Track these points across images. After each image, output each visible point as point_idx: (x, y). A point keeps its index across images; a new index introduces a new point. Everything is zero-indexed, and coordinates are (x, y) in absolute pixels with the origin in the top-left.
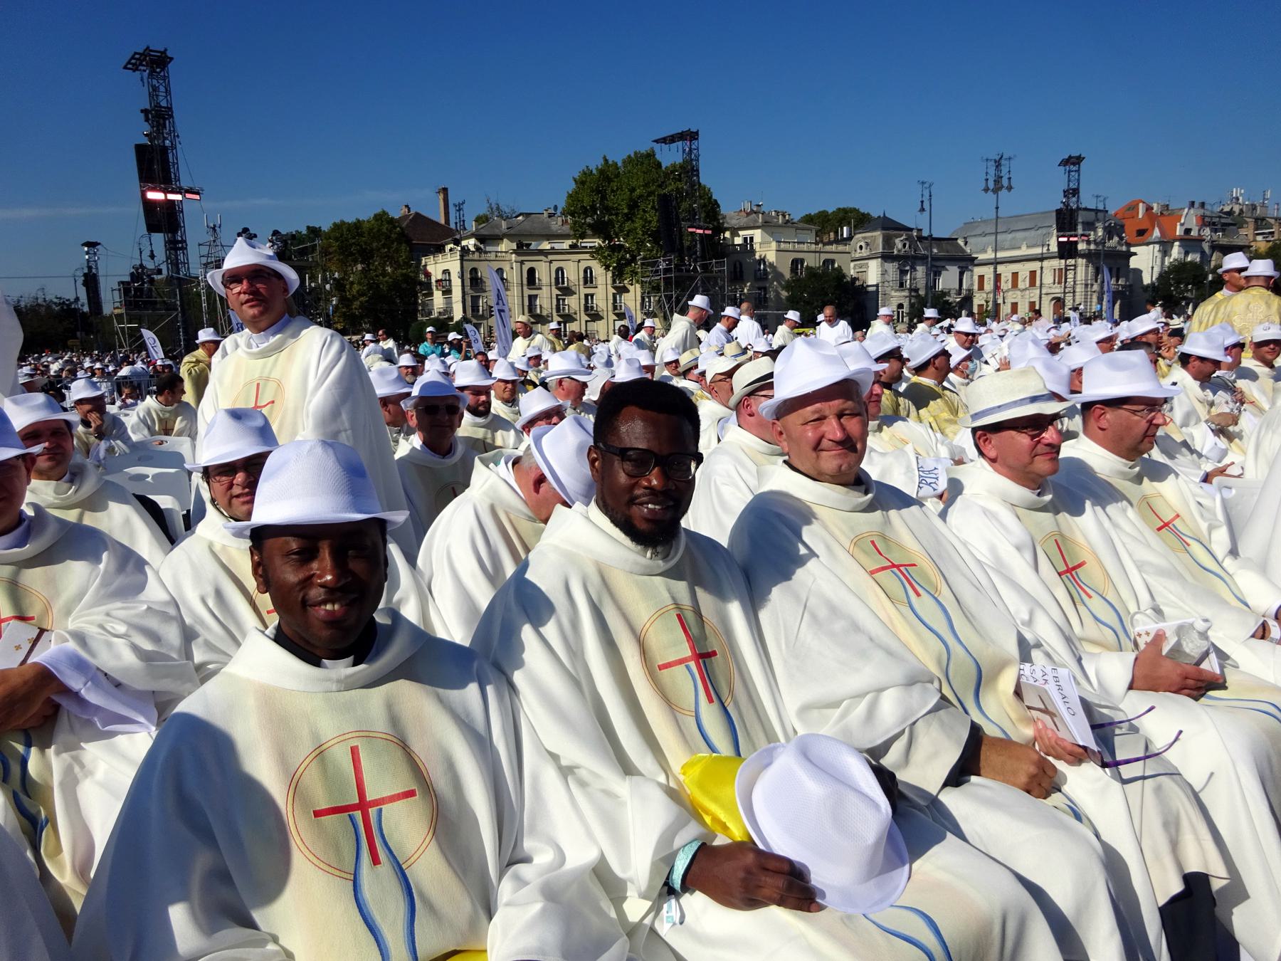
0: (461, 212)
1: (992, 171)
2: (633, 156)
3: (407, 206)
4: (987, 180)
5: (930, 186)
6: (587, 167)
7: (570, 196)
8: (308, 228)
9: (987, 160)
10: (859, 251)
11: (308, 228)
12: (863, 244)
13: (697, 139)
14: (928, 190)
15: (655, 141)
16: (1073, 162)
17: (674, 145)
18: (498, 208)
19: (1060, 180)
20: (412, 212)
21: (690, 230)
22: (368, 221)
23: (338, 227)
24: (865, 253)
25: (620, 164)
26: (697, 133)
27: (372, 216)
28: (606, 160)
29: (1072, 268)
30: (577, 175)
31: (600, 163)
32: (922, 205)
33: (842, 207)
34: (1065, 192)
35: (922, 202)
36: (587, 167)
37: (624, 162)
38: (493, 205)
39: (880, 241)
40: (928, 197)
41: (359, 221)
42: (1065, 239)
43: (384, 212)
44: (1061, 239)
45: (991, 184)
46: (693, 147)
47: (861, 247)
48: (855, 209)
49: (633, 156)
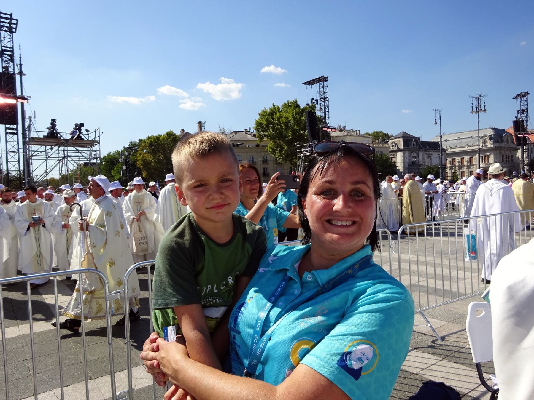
0: (204, 127)
1: (475, 102)
2: (287, 103)
3: (183, 130)
4: (472, 107)
5: (440, 111)
6: (265, 108)
7: (257, 122)
8: (139, 139)
9: (472, 97)
10: (392, 148)
11: (139, 139)
12: (394, 144)
13: (327, 81)
14: (439, 114)
15: (305, 84)
16: (523, 95)
17: (314, 86)
18: (224, 131)
19: (517, 105)
20: (185, 132)
21: (324, 129)
22: (164, 135)
23: (149, 138)
24: (395, 148)
25: (280, 107)
26: (327, 77)
27: (166, 133)
28: (274, 105)
29: (524, 150)
30: (260, 112)
31: (271, 106)
32: (436, 121)
33: (375, 131)
34: (518, 111)
35: (436, 119)
36: (265, 108)
37: (282, 105)
38: (222, 129)
39: (402, 142)
40: (439, 117)
41: (159, 135)
42: (522, 136)
43: (171, 131)
44: (519, 136)
45: (475, 109)
46: (325, 85)
47: (393, 146)
48: (381, 132)
49: (287, 103)
